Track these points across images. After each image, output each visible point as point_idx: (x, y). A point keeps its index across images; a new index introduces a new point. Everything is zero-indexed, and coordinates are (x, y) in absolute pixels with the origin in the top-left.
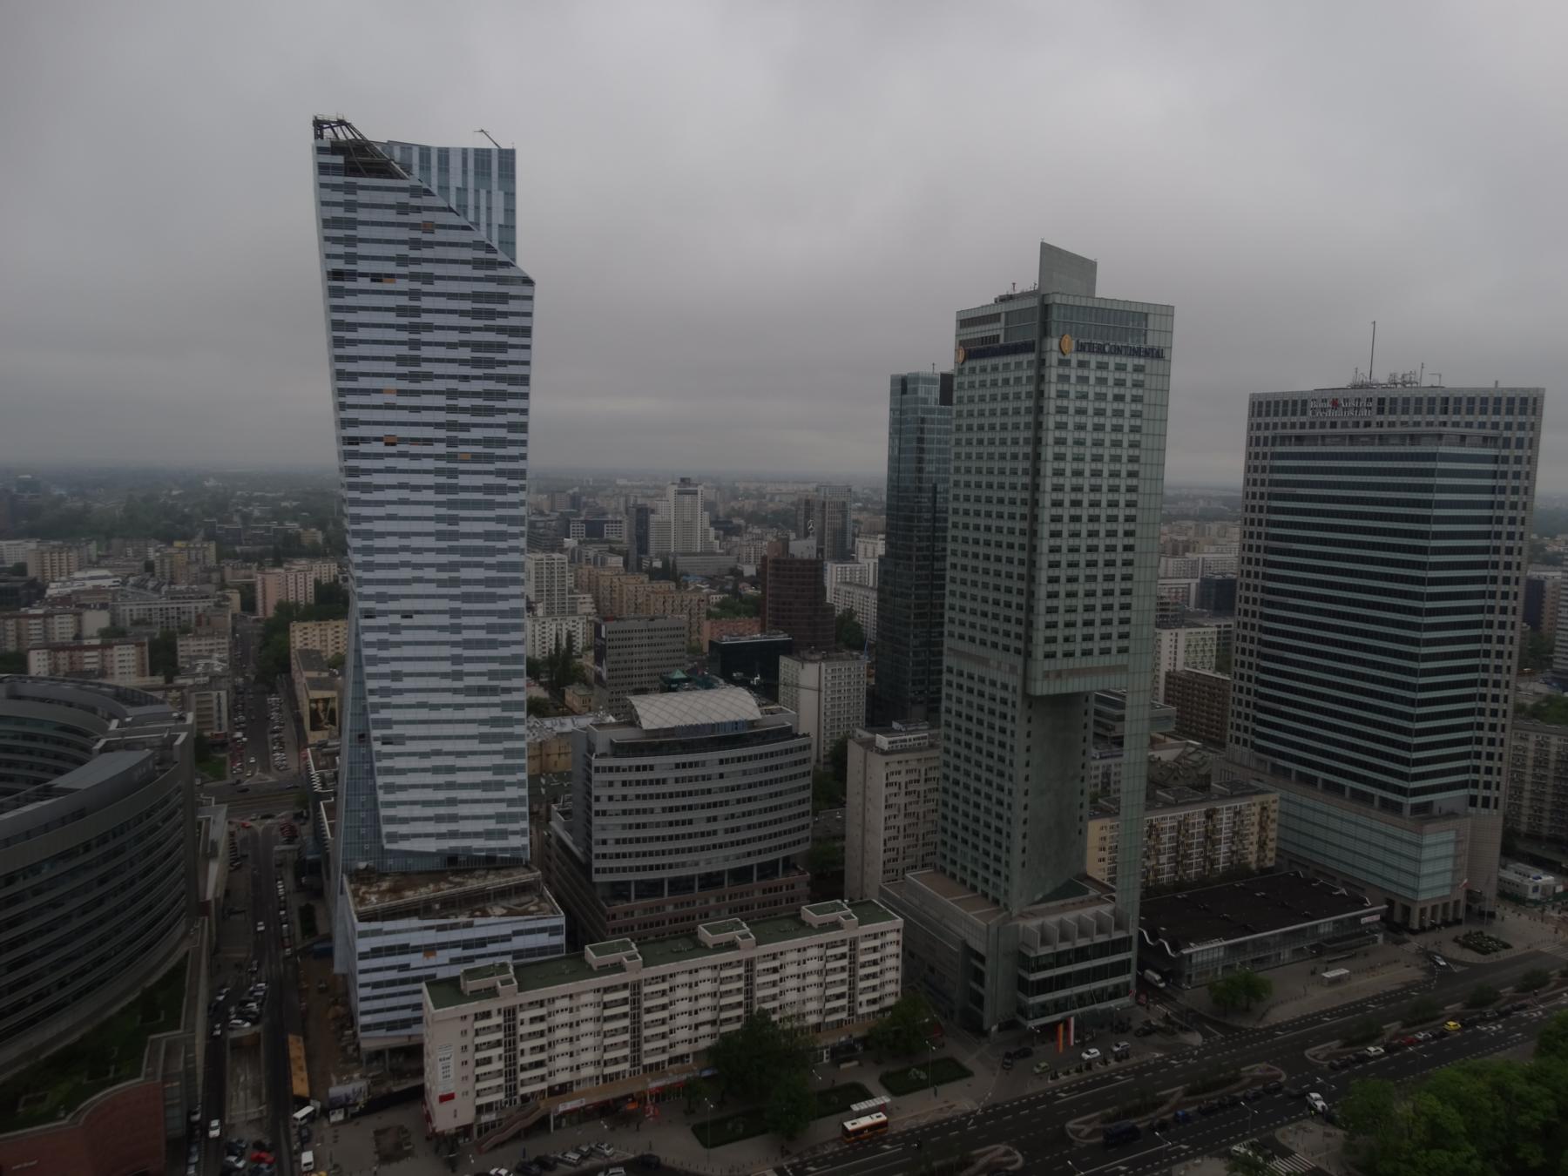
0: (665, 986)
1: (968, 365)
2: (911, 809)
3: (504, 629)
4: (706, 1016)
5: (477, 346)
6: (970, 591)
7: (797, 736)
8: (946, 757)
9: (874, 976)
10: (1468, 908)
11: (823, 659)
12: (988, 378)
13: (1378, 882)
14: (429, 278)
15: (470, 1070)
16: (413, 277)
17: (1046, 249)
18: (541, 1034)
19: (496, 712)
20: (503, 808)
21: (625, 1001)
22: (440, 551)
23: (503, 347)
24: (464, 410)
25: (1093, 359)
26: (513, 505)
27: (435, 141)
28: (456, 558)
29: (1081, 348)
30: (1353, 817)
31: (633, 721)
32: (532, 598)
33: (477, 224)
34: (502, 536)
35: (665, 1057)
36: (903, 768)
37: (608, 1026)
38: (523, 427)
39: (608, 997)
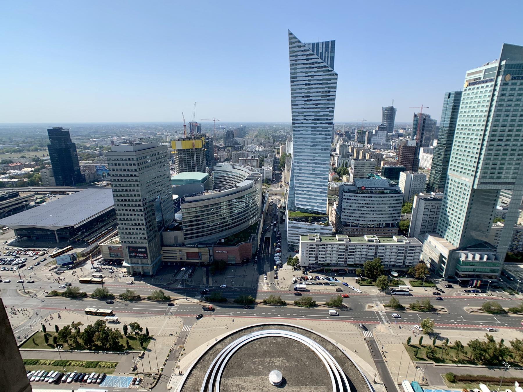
0: (354, 247)
4: (364, 256)
5: (323, 92)
6: (458, 157)
7: (399, 193)
9: (412, 256)
14: (312, 76)
15: (308, 255)
16: (309, 76)
18: (324, 251)
21: (344, 249)
22: (312, 142)
23: (329, 92)
24: (319, 108)
26: (329, 131)
27: (315, 42)
28: (315, 144)
33: (325, 61)
34: (326, 138)
35: (353, 263)
37: (340, 253)
38: (333, 112)
39: (340, 247)
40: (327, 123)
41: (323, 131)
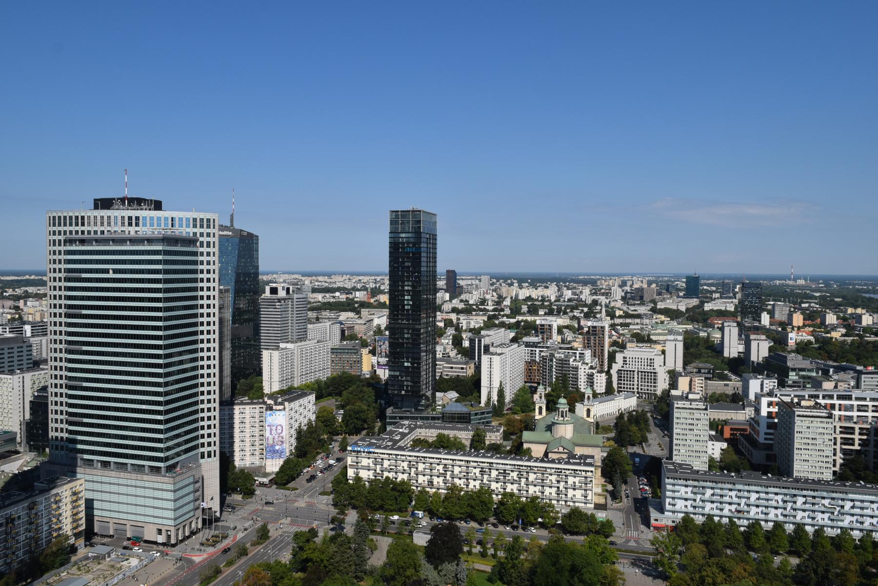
10: (204, 520)
13: (151, 520)
30: (133, 483)
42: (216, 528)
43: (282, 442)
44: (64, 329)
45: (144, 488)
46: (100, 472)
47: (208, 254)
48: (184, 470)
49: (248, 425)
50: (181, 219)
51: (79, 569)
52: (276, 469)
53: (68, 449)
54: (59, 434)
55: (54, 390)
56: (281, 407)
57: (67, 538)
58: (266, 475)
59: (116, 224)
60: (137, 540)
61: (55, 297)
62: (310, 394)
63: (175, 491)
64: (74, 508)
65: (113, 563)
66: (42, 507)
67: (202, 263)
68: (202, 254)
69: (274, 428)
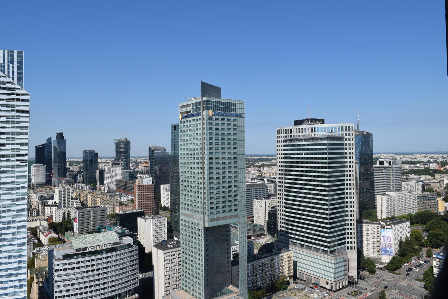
1: (183, 120)
2: (173, 269)
3: (18, 216)
5: (8, 117)
8: (182, 250)
10: (349, 282)
11: (152, 218)
12: (189, 124)
13: (323, 276)
17: (203, 84)
19: (15, 247)
20: (17, 283)
23: (18, 117)
25: (220, 118)
26: (22, 172)
29: (215, 114)
30: (315, 256)
31: (71, 247)
32: (57, 202)
36: (170, 254)
40: (17, 161)
41: (13, 172)
42: (356, 287)
43: (391, 247)
44: (284, 180)
45: (320, 260)
46: (299, 249)
47: (350, 144)
48: (339, 254)
49: (370, 235)
50: (335, 128)
51: (291, 293)
52: (388, 261)
53: (285, 236)
54: (282, 229)
55: (280, 208)
56: (390, 227)
57: (286, 277)
58: (382, 263)
59: (305, 131)
60: (316, 285)
61: (280, 166)
62: (407, 221)
63: (335, 264)
64: (289, 264)
65: (306, 294)
66: (276, 261)
67: (346, 149)
68: (346, 144)
69: (386, 238)
